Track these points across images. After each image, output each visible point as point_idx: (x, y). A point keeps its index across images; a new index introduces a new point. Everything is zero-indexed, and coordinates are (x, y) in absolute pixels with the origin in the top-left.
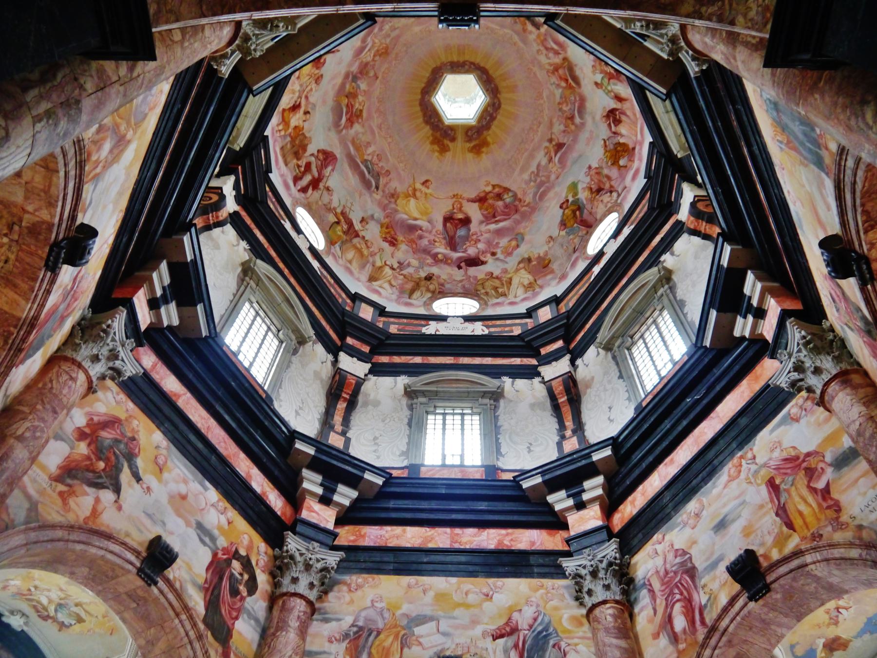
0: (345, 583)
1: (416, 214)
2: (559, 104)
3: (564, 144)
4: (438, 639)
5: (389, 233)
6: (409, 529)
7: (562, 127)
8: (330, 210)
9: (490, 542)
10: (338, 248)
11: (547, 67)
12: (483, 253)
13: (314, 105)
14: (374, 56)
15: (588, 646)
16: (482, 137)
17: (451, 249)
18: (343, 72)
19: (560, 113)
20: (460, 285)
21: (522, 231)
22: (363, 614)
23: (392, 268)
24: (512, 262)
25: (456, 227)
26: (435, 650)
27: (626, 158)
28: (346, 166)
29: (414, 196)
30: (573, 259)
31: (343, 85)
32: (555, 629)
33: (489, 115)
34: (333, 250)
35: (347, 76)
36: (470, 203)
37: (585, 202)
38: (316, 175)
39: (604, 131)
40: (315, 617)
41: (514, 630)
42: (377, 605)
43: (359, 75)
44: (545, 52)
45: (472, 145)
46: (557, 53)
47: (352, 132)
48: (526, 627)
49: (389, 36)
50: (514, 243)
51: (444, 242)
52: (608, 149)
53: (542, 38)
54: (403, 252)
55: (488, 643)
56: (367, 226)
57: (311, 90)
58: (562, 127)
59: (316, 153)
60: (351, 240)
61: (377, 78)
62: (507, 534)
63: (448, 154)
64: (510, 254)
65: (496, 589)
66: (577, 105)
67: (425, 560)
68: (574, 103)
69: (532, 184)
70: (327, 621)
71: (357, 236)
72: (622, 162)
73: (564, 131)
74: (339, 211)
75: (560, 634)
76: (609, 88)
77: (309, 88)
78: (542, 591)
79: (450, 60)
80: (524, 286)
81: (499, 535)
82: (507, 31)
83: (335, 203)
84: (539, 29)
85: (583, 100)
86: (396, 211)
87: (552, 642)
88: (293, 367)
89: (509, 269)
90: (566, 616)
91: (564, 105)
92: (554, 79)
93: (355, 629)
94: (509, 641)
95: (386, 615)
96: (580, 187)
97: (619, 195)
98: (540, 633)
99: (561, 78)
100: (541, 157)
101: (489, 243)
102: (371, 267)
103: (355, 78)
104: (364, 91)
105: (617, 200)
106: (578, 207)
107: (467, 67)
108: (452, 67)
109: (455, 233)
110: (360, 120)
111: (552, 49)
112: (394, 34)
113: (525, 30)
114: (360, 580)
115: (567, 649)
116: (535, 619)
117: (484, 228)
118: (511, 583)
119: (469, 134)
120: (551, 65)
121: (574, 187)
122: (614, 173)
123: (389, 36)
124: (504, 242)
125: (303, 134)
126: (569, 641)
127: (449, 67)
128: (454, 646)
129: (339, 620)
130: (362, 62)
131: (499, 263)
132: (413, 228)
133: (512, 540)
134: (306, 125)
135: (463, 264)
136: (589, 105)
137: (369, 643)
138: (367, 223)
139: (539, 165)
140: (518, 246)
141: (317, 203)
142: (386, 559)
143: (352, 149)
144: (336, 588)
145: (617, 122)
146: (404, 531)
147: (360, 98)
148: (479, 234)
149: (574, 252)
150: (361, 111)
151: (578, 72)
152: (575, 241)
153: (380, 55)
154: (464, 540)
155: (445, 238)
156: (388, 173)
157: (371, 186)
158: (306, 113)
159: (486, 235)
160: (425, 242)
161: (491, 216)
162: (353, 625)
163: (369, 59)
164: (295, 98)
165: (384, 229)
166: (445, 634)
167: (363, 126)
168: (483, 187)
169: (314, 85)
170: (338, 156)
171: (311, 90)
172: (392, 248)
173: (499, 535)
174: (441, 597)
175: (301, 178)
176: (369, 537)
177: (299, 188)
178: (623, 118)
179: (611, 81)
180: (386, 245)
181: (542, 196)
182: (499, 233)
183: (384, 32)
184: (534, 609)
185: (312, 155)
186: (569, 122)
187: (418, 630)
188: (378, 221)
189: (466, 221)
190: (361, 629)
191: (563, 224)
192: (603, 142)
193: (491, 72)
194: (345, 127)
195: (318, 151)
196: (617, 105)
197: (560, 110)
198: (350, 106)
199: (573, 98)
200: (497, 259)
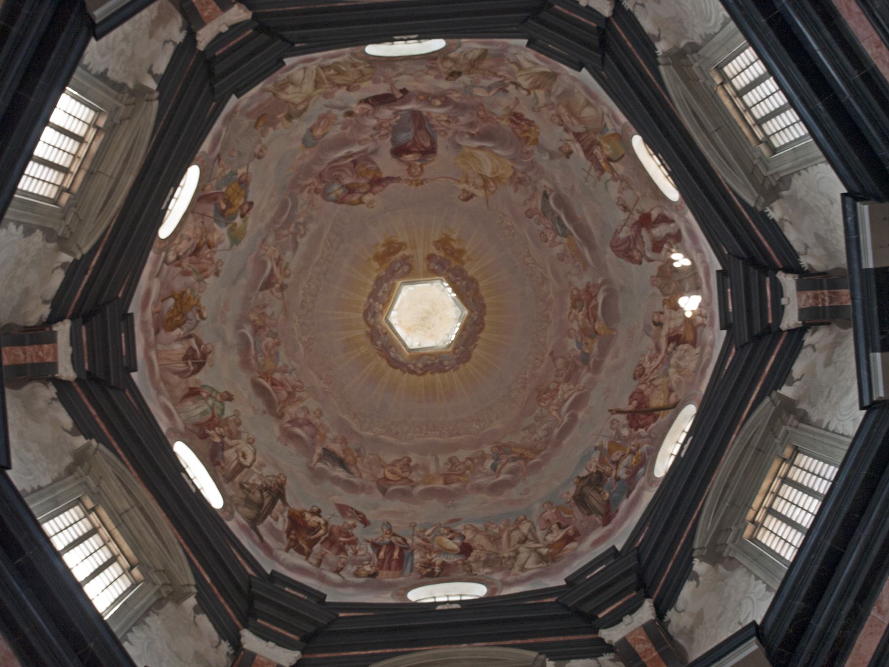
1: (481, 154)
2: (278, 344)
3: (261, 290)
5: (524, 132)
7: (268, 311)
8: (622, 179)
10: (610, 127)
11: (304, 394)
12: (367, 114)
13: (646, 331)
14: (557, 390)
16: (387, 265)
17: (420, 113)
18: (602, 375)
19: (274, 330)
20: (401, 70)
21: (308, 152)
23: (518, 85)
24: (318, 107)
25: (415, 143)
27: (166, 310)
28: (596, 233)
29: (485, 179)
30: (220, 145)
31: (603, 353)
33: (382, 297)
34: (619, 128)
35: (597, 368)
36: (396, 176)
37: (215, 225)
38: (644, 232)
39: (205, 332)
43: (579, 363)
44: (311, 417)
45: (401, 253)
46: (294, 422)
47: (587, 278)
49: (537, 419)
50: (318, 132)
51: (433, 122)
52: (194, 309)
53: (318, 437)
54: (501, 105)
56: (561, 144)
57: (651, 359)
58: (268, 311)
59: (644, 261)
60: (587, 132)
61: (551, 354)
63: (437, 238)
64: (322, 117)
66: (253, 351)
68: (257, 353)
69: (301, 220)
71: (577, 136)
72: (171, 301)
73: (264, 307)
74: (608, 175)
76: (210, 401)
77: (655, 363)
79: (446, 375)
80: (292, 83)
82: (369, 434)
83: (614, 187)
84: (325, 449)
85: (245, 363)
86: (513, 160)
88: (700, 30)
89: (322, 99)
91: (270, 344)
92: (291, 378)
96: (227, 242)
97: (165, 261)
99: (282, 385)
100: (293, 260)
101: (360, 128)
102: (553, 90)
103: (585, 359)
104: (570, 337)
105: (167, 252)
106: (223, 216)
107: (420, 365)
108: (441, 363)
109: (415, 134)
110: (575, 292)
111: (300, 426)
112: (529, 420)
113: (344, 441)
117: (370, 146)
119: (406, 268)
120: (301, 399)
121: (235, 240)
122: (178, 284)
123: (537, 419)
124: (335, 131)
125: (664, 295)
127: (446, 363)
130: (576, 383)
131: (339, 103)
132: (484, 136)
134: (659, 307)
135: (399, 95)
136: (235, 358)
138: (560, 149)
139: (295, 249)
140: (311, 130)
141: (644, 195)
143: (587, 255)
145: (190, 355)
147: (575, 326)
148: (377, 137)
149: (219, 157)
150: (574, 307)
151: (259, 403)
152: (220, 170)
153: (548, 389)
155: (432, 126)
156: (529, 214)
157: (555, 199)
158: (659, 324)
159: (364, 136)
160: (463, 119)
161: (358, 162)
163: (564, 387)
164: (676, 355)
165: (532, 138)
167: (570, 284)
168: (376, 199)
169: (647, 365)
170: (609, 249)
171: (651, 359)
172: (518, 110)
175: (669, 235)
177: (672, 225)
178: (181, 366)
179: (209, 416)
180: (529, 115)
181: (283, 207)
182: (344, 142)
183: (545, 426)
185: (650, 260)
186: (259, 323)
188: (543, 149)
189: (398, 151)
191: (243, 183)
192: (205, 315)
193: (384, 363)
194: (598, 287)
195: (640, 263)
196: (192, 381)
197: (275, 335)
198: (591, 316)
199: (260, 359)
200: (341, 108)
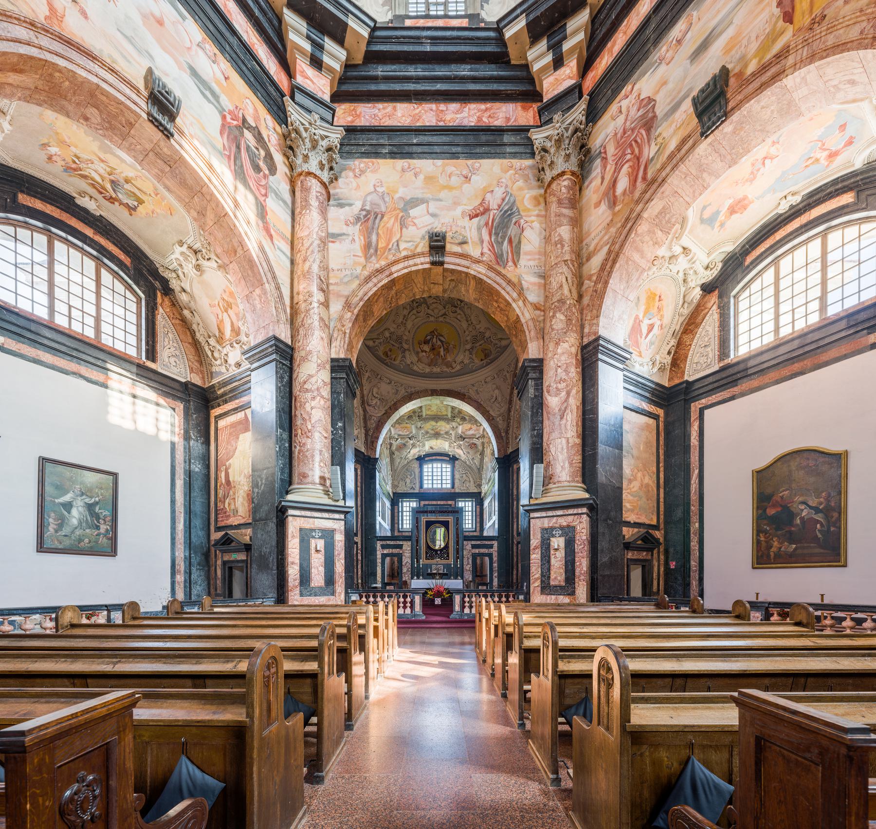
0: (350, 169)
4: (428, 219)
6: (399, 105)
9: (471, 120)
15: (540, 223)
22: (369, 198)
26: (426, 229)
32: (517, 208)
40: (331, 202)
41: (487, 210)
42: (380, 190)
48: (496, 207)
55: (466, 222)
62: (487, 109)
65: (474, 171)
67: (415, 141)
70: (341, 206)
75: (521, 213)
78: (512, 172)
81: (479, 110)
87: (514, 220)
90: (527, 196)
93: (364, 213)
94: (481, 220)
95: (387, 199)
98: (506, 212)
114: (362, 165)
115: (525, 226)
116: (503, 200)
118: (486, 163)
126: (527, 219)
128: (440, 226)
129: (350, 205)
133: (490, 116)
137: (376, 225)
142: (382, 141)
144: (343, 174)
146: (394, 108)
154: (448, 117)
162: (362, 210)
166: (434, 215)
173: (479, 110)
174: (430, 179)
176: (364, 117)
184: (503, 189)
187: (413, 212)
190: (369, 212)
